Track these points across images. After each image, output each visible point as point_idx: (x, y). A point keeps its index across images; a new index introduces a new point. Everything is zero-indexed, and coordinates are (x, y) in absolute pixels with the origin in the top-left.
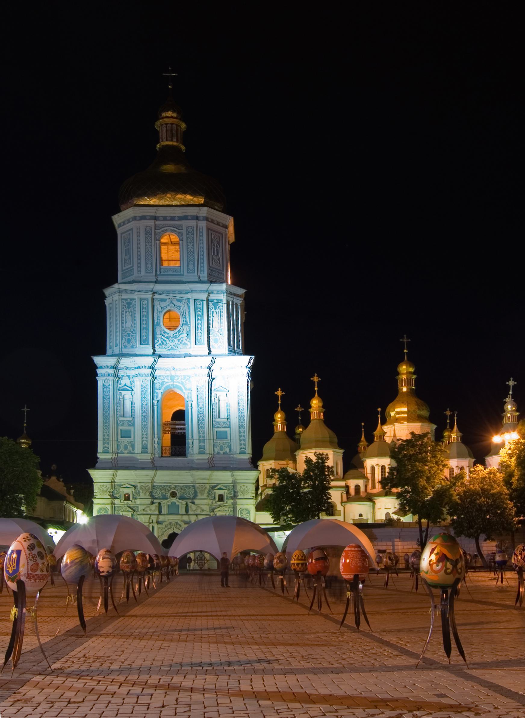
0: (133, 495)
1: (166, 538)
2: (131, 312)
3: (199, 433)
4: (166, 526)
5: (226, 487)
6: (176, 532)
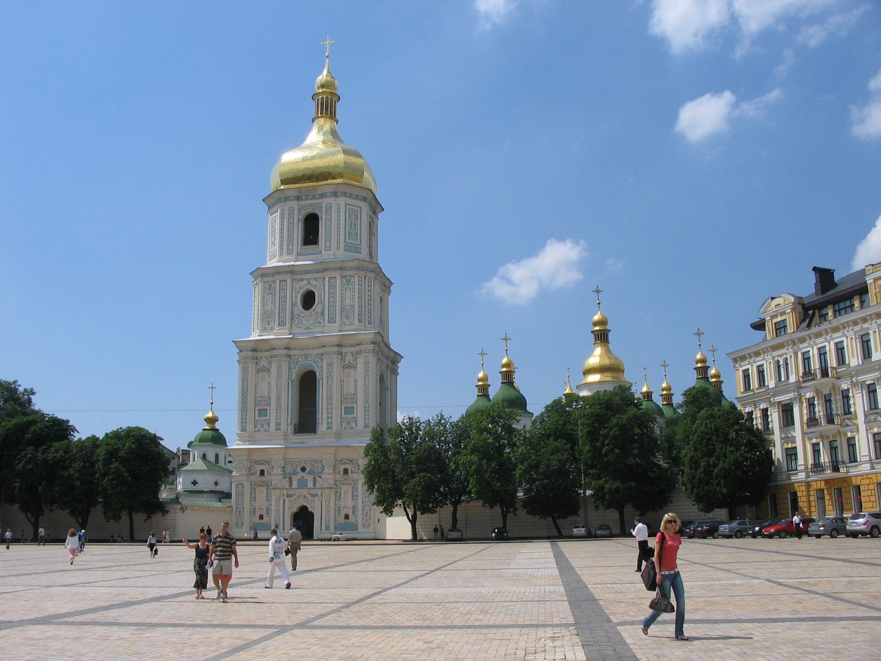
0: (267, 471)
1: (295, 510)
2: (272, 294)
3: (328, 409)
4: (295, 500)
5: (350, 461)
6: (304, 504)
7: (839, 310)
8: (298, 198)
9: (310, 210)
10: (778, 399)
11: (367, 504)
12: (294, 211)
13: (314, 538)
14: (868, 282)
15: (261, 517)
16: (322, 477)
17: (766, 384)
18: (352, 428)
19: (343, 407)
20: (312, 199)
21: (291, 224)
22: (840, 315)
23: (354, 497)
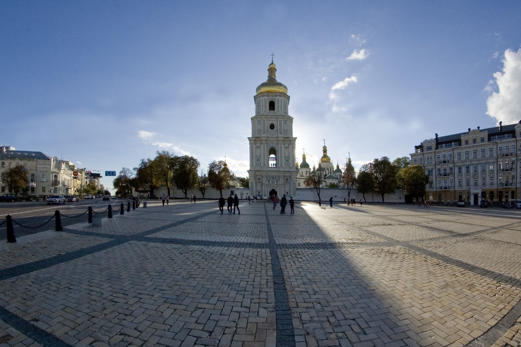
7: (446, 146)
8: (268, 96)
9: (272, 100)
10: (427, 168)
15: (259, 192)
16: (280, 181)
18: (288, 166)
21: (265, 103)
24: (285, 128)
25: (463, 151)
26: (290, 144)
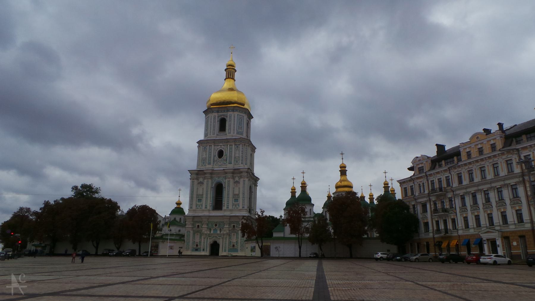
7: (447, 163)
8: (218, 112)
9: (223, 117)
10: (420, 200)
11: (242, 241)
12: (216, 117)
13: (219, 255)
14: (461, 151)
15: (197, 245)
16: (224, 229)
17: (414, 194)
18: (237, 208)
19: (234, 199)
20: (223, 112)
22: (448, 165)
23: (237, 238)
24: (237, 155)
25: (463, 170)
26: (241, 177)
